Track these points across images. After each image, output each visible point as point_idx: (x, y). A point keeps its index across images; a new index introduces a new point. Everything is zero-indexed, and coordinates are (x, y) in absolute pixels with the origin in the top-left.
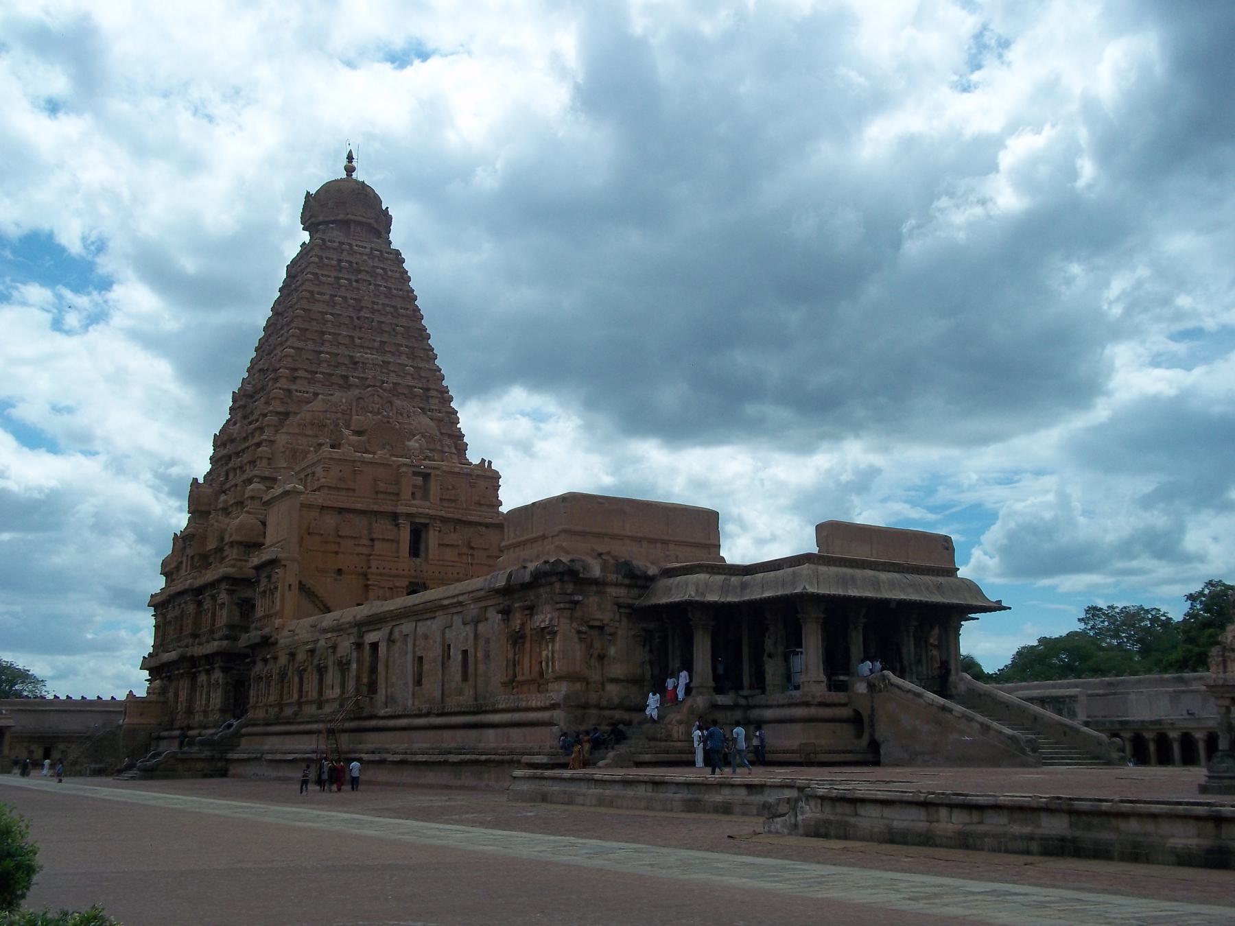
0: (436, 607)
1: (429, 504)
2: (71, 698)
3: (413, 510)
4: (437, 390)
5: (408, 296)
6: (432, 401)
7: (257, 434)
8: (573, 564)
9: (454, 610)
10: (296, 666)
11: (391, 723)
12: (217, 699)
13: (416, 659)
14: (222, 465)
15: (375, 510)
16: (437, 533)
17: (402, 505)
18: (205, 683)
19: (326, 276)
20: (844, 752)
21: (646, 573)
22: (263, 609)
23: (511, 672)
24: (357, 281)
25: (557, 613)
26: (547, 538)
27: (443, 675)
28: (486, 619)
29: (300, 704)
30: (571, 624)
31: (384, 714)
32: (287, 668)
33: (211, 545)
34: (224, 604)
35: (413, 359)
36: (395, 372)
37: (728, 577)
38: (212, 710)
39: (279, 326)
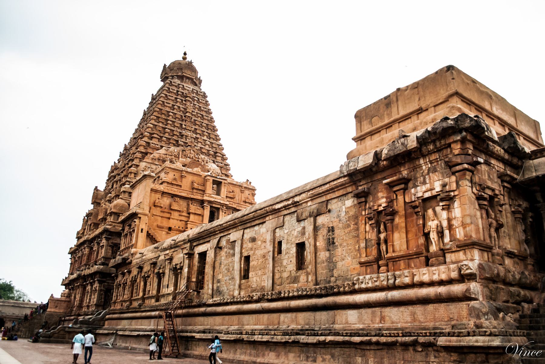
0: (268, 213)
3: (212, 200)
6: (217, 158)
9: (286, 212)
10: (143, 274)
11: (220, 309)
12: (95, 299)
15: (192, 197)
16: (223, 213)
17: (206, 196)
18: (89, 291)
19: (170, 96)
23: (374, 252)
24: (185, 101)
25: (453, 178)
26: (427, 110)
27: (274, 267)
28: (329, 211)
31: (212, 303)
33: (100, 217)
34: (103, 246)
35: (210, 139)
38: (92, 305)
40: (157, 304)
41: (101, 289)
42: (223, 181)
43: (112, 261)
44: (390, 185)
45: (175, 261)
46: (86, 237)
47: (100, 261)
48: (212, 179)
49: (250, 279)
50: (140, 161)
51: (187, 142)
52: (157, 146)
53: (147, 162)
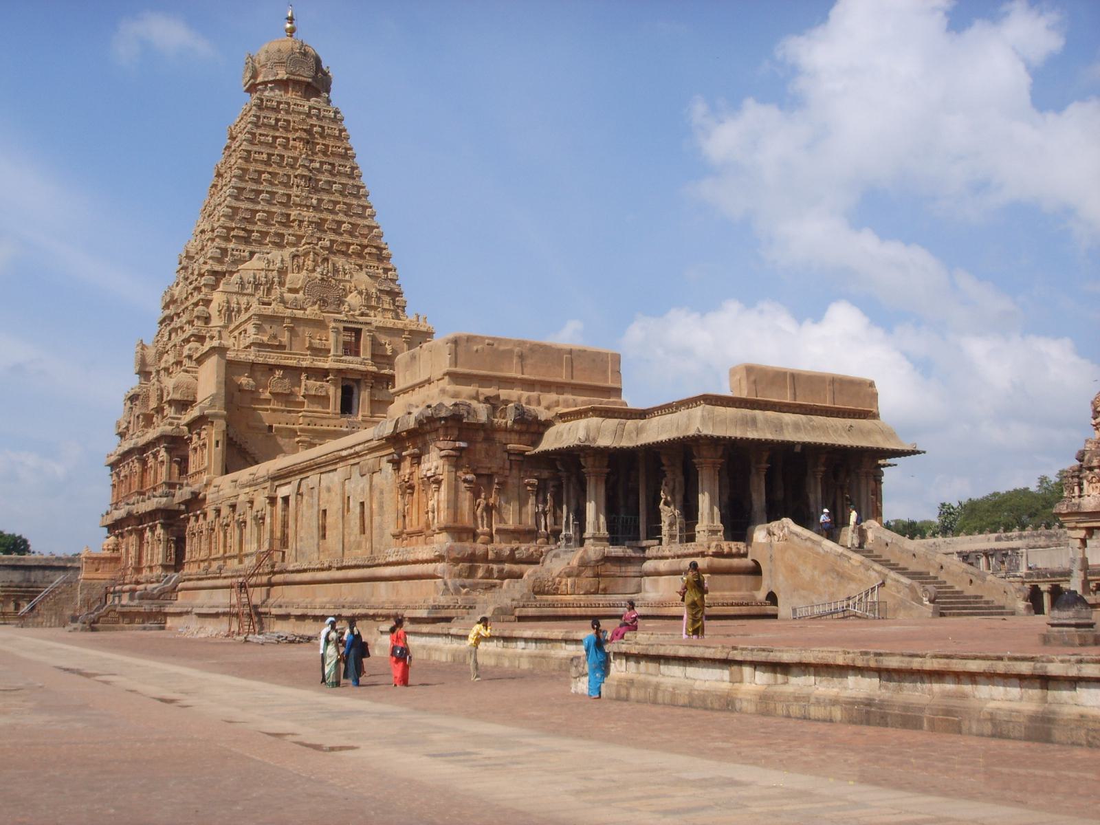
0: (337, 459)
4: (375, 247)
7: (195, 294)
8: (457, 408)
9: (352, 461)
12: (156, 552)
13: (321, 512)
14: (165, 326)
19: (263, 135)
20: (742, 605)
21: (536, 417)
24: (294, 140)
27: (343, 528)
28: (380, 470)
29: (225, 558)
30: (456, 473)
32: (214, 524)
34: (162, 462)
36: (333, 229)
37: (624, 420)
38: (155, 566)
39: (219, 188)
40: (241, 566)
41: (168, 539)
42: (365, 328)
43: (178, 493)
44: (413, 456)
47: (160, 491)
48: (341, 326)
49: (327, 540)
52: (242, 253)
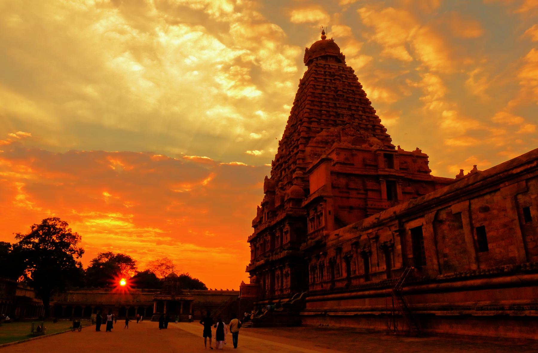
1: (394, 170)
2: (217, 290)
3: (387, 173)
5: (358, 86)
6: (377, 131)
9: (529, 176)
10: (343, 255)
11: (459, 284)
12: (287, 282)
13: (475, 230)
16: (400, 186)
18: (280, 275)
22: (313, 228)
24: (334, 80)
27: (524, 236)
32: (335, 258)
33: (277, 204)
34: (287, 231)
38: (286, 288)
40: (369, 283)
43: (304, 245)
45: (382, 239)
46: (267, 225)
48: (382, 153)
50: (305, 146)
51: (344, 120)
53: (312, 146)
